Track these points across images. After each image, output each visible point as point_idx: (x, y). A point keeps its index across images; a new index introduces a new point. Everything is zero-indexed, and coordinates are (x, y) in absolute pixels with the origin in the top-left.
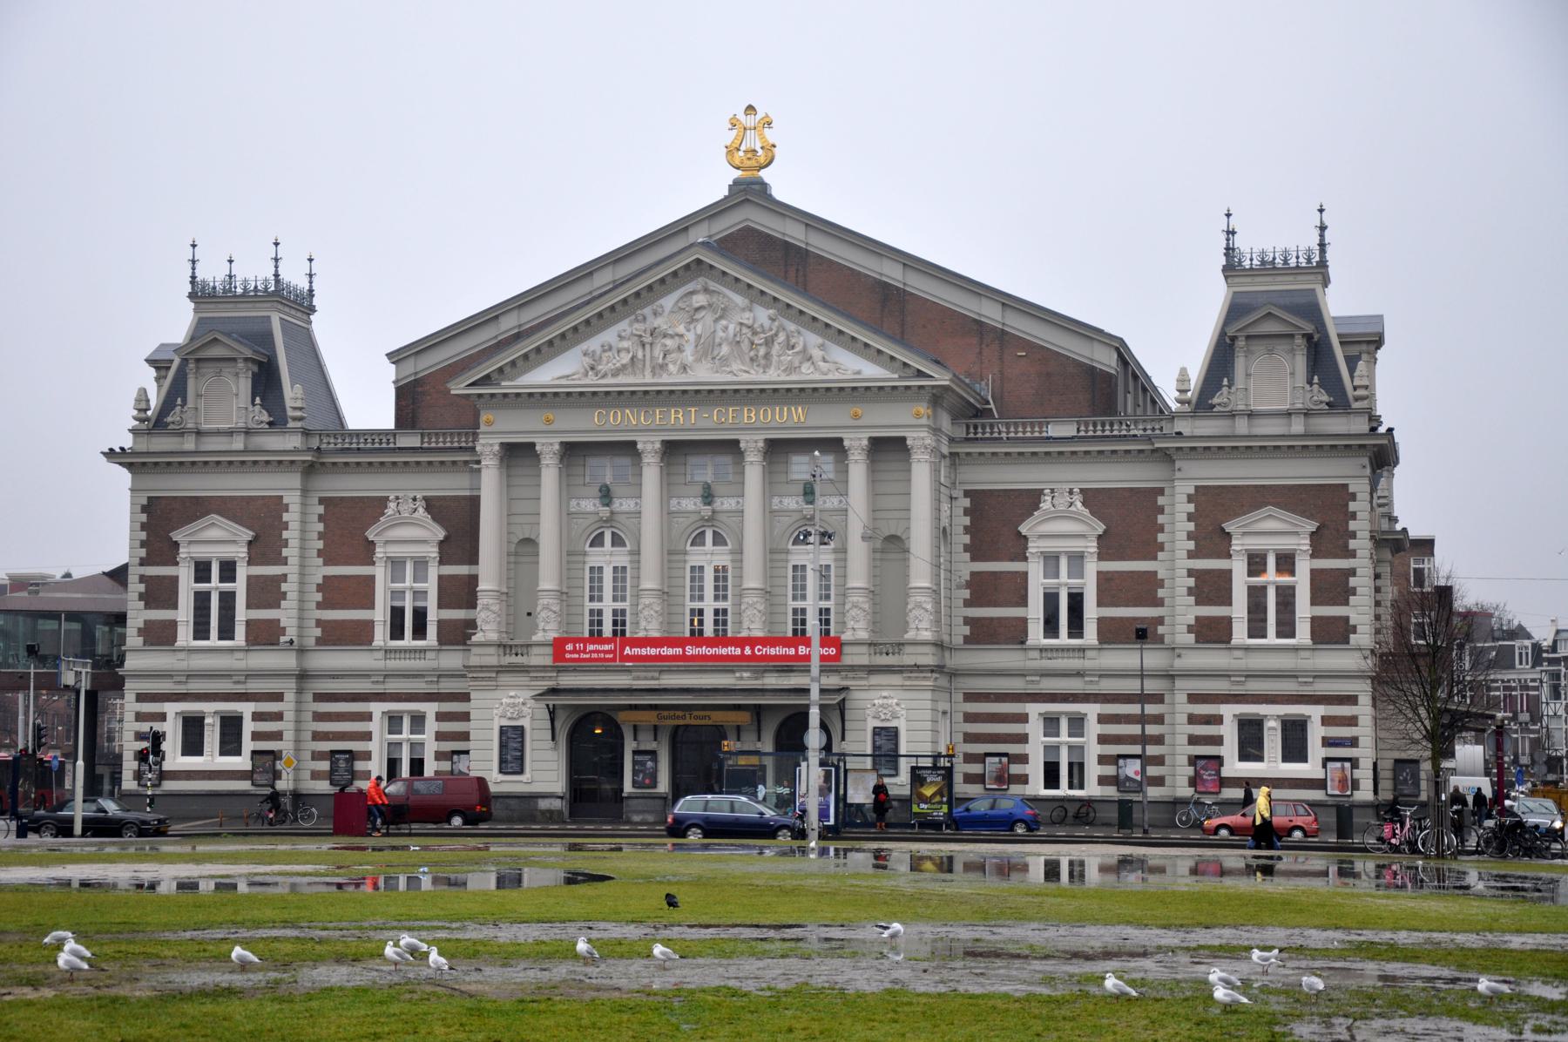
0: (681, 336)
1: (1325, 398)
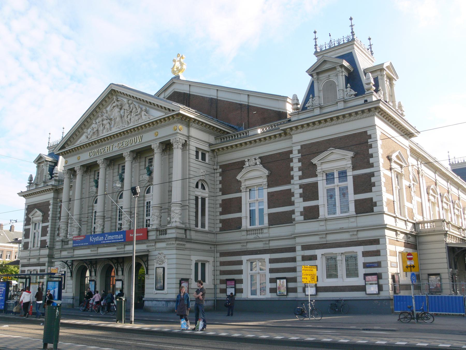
1: (353, 92)
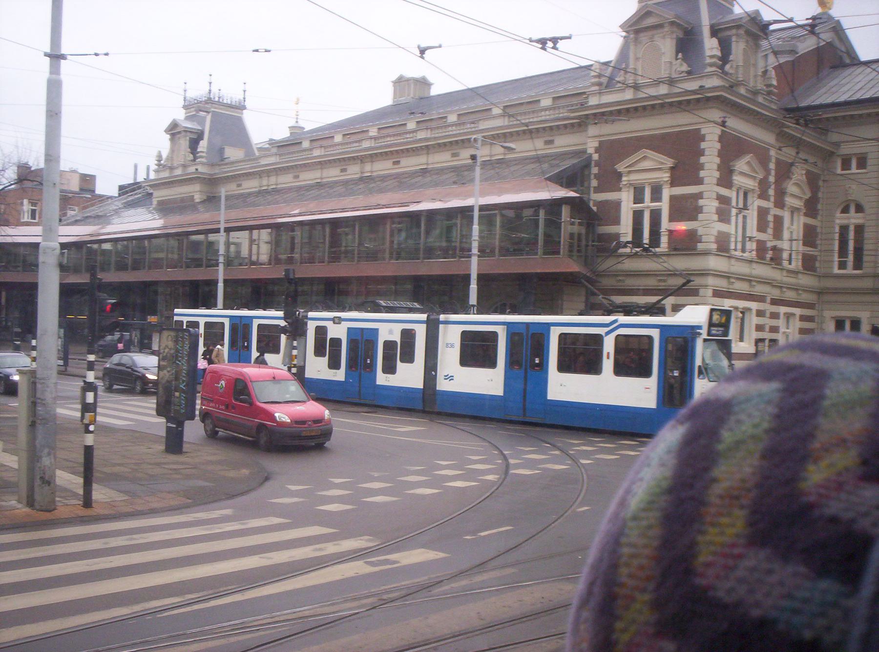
1: (685, 67)
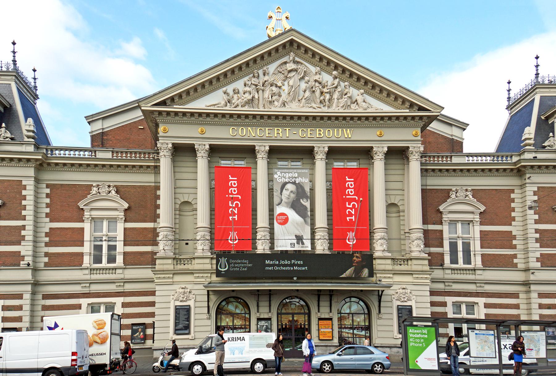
0: (280, 87)
